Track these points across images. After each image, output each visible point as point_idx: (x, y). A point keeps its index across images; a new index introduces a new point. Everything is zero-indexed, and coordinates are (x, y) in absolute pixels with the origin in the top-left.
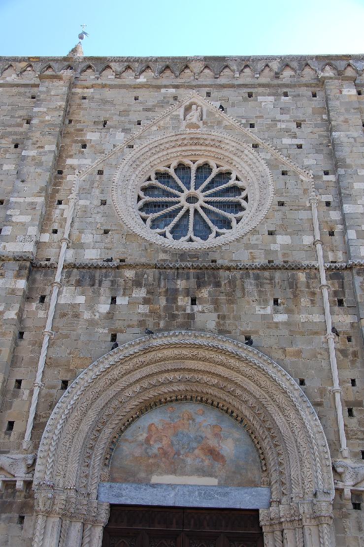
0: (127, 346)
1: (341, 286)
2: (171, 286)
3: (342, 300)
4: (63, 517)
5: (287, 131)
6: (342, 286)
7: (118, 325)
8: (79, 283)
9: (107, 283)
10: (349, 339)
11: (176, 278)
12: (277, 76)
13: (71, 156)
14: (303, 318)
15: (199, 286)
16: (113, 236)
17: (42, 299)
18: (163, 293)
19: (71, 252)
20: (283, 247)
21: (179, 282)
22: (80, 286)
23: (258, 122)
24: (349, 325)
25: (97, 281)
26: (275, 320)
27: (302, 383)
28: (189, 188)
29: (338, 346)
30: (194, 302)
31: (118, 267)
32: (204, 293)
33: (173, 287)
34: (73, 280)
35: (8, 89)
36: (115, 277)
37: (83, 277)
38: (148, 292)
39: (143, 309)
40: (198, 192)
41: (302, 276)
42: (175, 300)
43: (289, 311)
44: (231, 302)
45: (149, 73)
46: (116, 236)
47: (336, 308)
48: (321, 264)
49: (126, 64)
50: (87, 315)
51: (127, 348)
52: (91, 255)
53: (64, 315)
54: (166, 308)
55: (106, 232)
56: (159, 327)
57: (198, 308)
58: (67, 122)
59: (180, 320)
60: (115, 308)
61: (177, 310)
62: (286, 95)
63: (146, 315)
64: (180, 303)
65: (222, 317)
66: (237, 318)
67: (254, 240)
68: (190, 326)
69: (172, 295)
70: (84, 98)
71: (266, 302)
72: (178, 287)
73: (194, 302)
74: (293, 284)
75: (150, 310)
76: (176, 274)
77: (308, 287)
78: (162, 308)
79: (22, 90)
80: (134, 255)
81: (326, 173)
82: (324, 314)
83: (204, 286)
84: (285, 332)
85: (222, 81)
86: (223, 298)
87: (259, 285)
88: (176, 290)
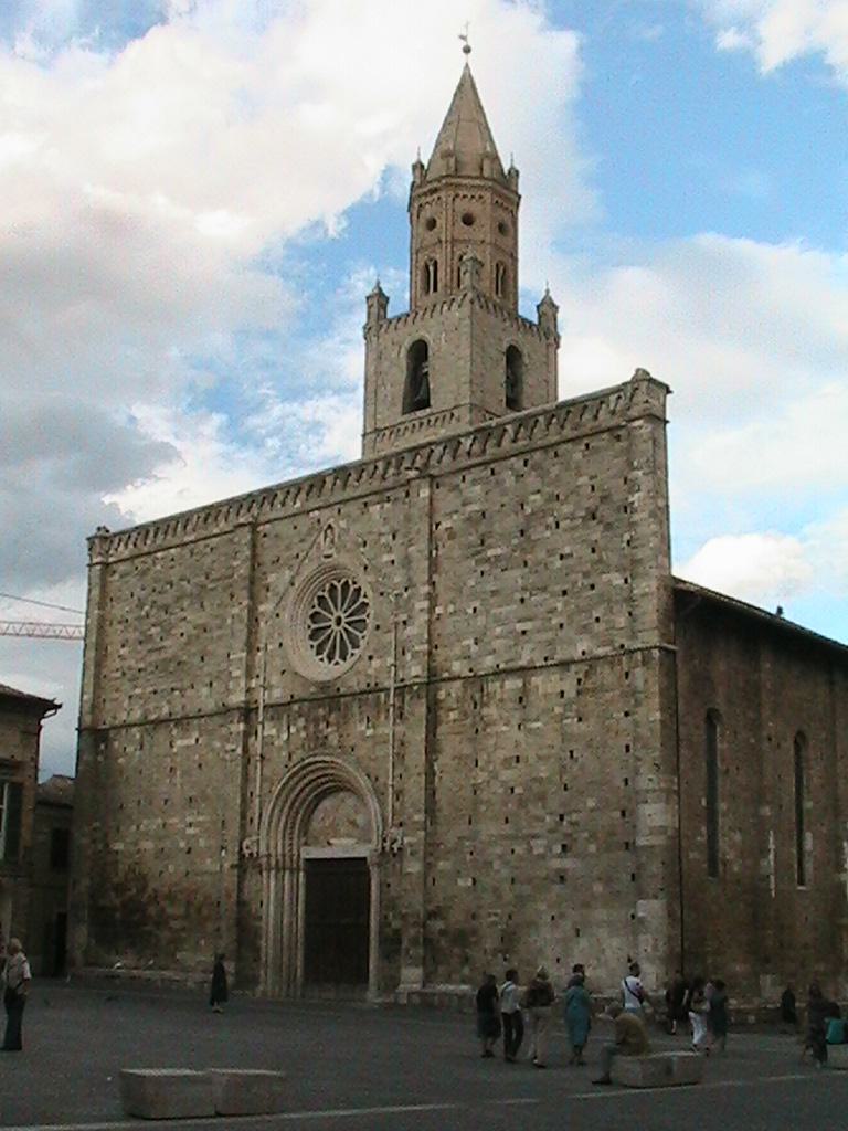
7: (292, 747)
9: (285, 716)
12: (383, 478)
13: (261, 603)
14: (380, 731)
15: (330, 712)
20: (376, 669)
23: (369, 539)
28: (330, 620)
30: (327, 726)
31: (289, 703)
32: (332, 718)
38: (306, 720)
39: (303, 734)
41: (383, 695)
43: (374, 727)
45: (303, 495)
47: (398, 721)
48: (390, 684)
49: (286, 490)
52: (277, 695)
57: (330, 730)
65: (341, 736)
67: (360, 666)
69: (316, 722)
70: (265, 535)
73: (327, 726)
79: (229, 536)
80: (299, 694)
81: (406, 589)
85: (350, 493)
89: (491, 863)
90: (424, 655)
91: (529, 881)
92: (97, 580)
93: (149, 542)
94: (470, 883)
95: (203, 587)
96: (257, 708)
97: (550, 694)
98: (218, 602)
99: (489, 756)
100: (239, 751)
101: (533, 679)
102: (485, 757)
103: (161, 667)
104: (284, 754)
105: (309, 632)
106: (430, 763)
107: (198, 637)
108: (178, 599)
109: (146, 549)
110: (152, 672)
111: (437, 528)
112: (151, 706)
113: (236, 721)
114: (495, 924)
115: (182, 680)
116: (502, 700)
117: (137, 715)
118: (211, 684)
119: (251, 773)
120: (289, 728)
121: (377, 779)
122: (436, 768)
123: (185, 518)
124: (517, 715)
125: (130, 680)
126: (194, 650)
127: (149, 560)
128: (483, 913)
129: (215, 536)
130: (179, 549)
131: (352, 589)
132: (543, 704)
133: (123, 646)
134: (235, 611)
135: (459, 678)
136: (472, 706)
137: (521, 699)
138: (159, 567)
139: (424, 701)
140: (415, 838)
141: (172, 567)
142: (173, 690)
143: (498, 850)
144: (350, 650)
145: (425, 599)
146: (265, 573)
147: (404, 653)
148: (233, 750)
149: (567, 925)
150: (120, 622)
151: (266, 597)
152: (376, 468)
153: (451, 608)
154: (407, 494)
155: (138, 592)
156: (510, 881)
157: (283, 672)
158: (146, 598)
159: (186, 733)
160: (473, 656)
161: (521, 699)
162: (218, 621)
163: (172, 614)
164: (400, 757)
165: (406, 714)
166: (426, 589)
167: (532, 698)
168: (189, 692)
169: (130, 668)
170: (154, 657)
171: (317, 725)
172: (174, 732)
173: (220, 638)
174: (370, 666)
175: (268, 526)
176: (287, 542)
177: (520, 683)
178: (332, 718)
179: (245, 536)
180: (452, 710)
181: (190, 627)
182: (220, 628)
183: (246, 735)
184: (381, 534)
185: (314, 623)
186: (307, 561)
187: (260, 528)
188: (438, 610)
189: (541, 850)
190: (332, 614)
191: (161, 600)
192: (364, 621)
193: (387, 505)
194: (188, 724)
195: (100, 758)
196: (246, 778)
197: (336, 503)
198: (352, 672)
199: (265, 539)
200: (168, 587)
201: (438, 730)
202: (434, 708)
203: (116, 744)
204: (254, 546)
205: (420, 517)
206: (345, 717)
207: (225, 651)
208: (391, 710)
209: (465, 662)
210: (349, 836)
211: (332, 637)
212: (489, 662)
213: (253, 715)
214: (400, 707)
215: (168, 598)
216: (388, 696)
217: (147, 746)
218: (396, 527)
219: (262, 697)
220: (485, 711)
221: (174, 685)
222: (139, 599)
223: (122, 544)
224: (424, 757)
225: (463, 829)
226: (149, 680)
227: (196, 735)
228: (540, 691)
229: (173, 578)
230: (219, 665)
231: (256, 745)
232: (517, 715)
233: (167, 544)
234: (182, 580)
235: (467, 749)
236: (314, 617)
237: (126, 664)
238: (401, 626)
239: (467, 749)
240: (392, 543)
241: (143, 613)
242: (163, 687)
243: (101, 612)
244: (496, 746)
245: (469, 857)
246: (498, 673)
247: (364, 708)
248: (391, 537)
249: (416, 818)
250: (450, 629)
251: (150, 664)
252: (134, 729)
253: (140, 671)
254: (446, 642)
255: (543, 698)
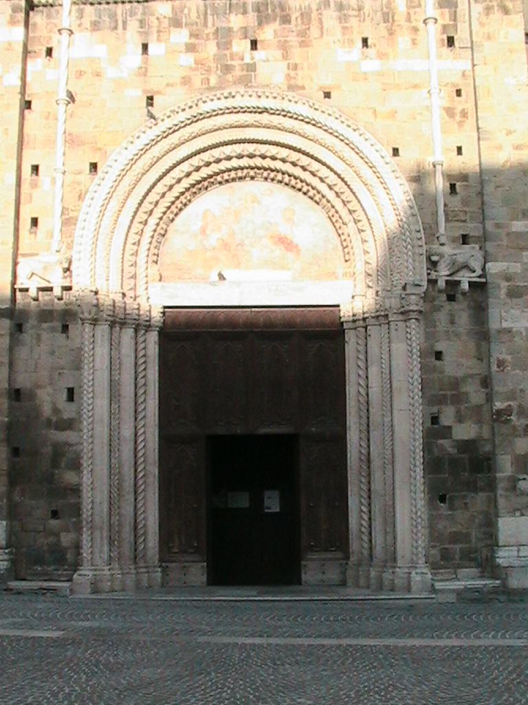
0: (168, 114)
1: (453, 18)
2: (221, 23)
3: (453, 38)
6: (454, 17)
7: (154, 84)
8: (96, 26)
10: (459, 93)
11: (228, 11)
15: (260, 24)
17: (49, 52)
18: (211, 36)
21: (233, 17)
22: (98, 30)
24: (461, 74)
25: (120, 23)
32: (267, 34)
33: (224, 25)
34: (87, 22)
36: (144, 14)
37: (100, 18)
38: (191, 35)
42: (228, 45)
43: (382, 56)
44: (304, 44)
50: (111, 73)
51: (169, 117)
53: (80, 74)
54: (217, 58)
56: (208, 83)
57: (259, 54)
60: (147, 59)
61: (232, 59)
63: (191, 69)
68: (251, 82)
69: (224, 37)
71: (351, 42)
72: (231, 25)
73: (254, 44)
75: (195, 60)
76: (228, 5)
77: (409, 19)
78: (211, 57)
82: (429, 57)
83: (268, 23)
86: (293, 39)
87: (343, 19)
88: (230, 30)
206: (303, 34)
247: (353, 22)
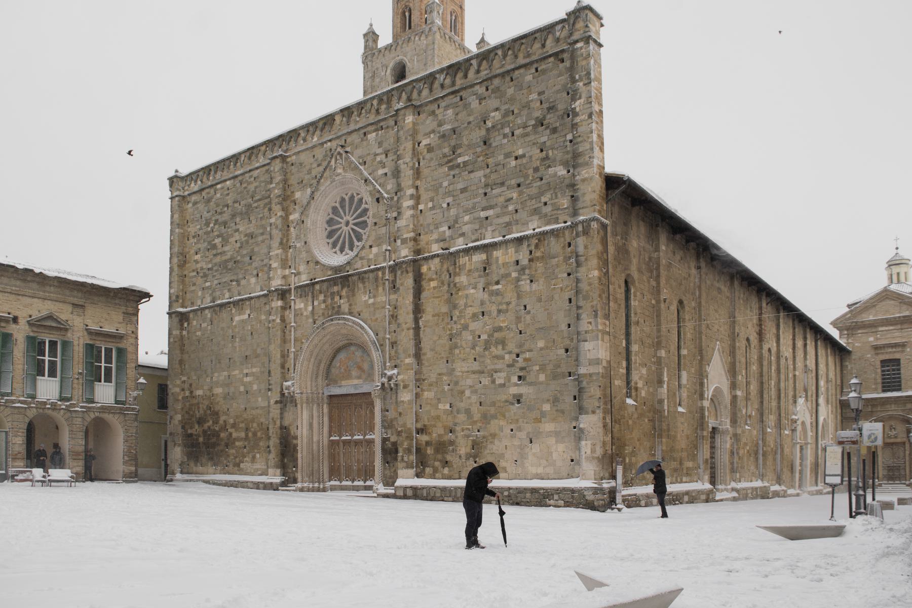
2: (332, 291)
4: (307, 403)
5: (381, 162)
15: (342, 289)
16: (311, 264)
19: (297, 278)
23: (369, 159)
26: (369, 303)
27: (377, 335)
29: (391, 313)
30: (340, 299)
32: (344, 293)
35: (261, 169)
38: (325, 296)
39: (323, 306)
40: (345, 218)
41: (380, 273)
42: (334, 298)
43: (374, 297)
44: (354, 295)
45: (318, 132)
46: (312, 264)
47: (391, 291)
52: (304, 280)
54: (331, 305)
55: (308, 262)
57: (342, 301)
58: (287, 186)
59: (336, 309)
62: (382, 128)
64: (335, 300)
65: (350, 305)
66: (356, 304)
67: (363, 253)
70: (292, 165)
71: (366, 292)
73: (340, 299)
74: (376, 279)
79: (267, 167)
84: (372, 309)
85: (352, 127)
86: (351, 293)
88: (334, 292)
89: (463, 392)
90: (410, 241)
91: (493, 404)
92: (177, 208)
93: (211, 178)
94: (448, 407)
95: (250, 206)
96: (290, 289)
97: (508, 263)
98: (261, 215)
99: (460, 312)
100: (278, 321)
101: (495, 252)
102: (458, 313)
103: (224, 265)
104: (311, 320)
105: (326, 233)
106: (416, 320)
107: (247, 242)
108: (233, 216)
109: (210, 184)
110: (216, 271)
111: (419, 146)
112: (218, 293)
113: (275, 298)
114: (468, 436)
115: (237, 274)
116: (470, 271)
117: (207, 302)
118: (258, 275)
119: (287, 337)
120: (313, 302)
121: (377, 335)
122: (421, 324)
123: (235, 158)
124: (482, 280)
125: (202, 277)
126: (245, 252)
127: (212, 191)
128: (458, 428)
129: (257, 168)
130: (232, 181)
131: (356, 199)
132: (502, 271)
133: (197, 254)
134: (273, 220)
135: (438, 256)
136: (448, 277)
137: (485, 269)
138: (218, 195)
139: (411, 275)
140: (407, 376)
141: (228, 194)
142: (231, 281)
143: (469, 382)
144: (356, 243)
145: (410, 199)
146: (293, 192)
147: (395, 241)
148: (274, 320)
149: (523, 435)
150: (194, 237)
151: (295, 209)
152: (372, 105)
153: (430, 205)
154: (396, 124)
155: (206, 215)
156: (478, 403)
157: (308, 262)
158: (211, 219)
159: (241, 311)
160: (448, 239)
161: (485, 269)
162: (261, 231)
163: (228, 228)
164: (394, 317)
165: (397, 286)
166: (411, 191)
167: (494, 267)
168: (243, 282)
169: (202, 269)
170: (218, 259)
171: (333, 299)
172: (233, 312)
173: (263, 241)
174: (371, 252)
175: (294, 157)
176: (308, 167)
177: (484, 256)
178: (344, 293)
179: (277, 166)
180: (433, 280)
181: (242, 236)
182: (262, 234)
183: (284, 308)
184: (376, 155)
185: (329, 226)
186: (322, 181)
187: (289, 160)
188: (421, 207)
189: (502, 381)
190: (342, 218)
191: (222, 219)
192: (366, 221)
193: (380, 132)
194: (242, 304)
195: (184, 333)
196: (284, 341)
197: (343, 135)
198: (358, 259)
199: (293, 167)
200: (226, 209)
201: (421, 297)
202: (418, 279)
203: (195, 323)
204: (285, 174)
205: (406, 138)
206: (353, 291)
207: (266, 251)
208: (387, 282)
209: (442, 245)
210: (359, 378)
211: (343, 235)
212: (459, 245)
213: (288, 295)
214: (392, 281)
215: (226, 217)
216: (384, 274)
217: (215, 322)
218: (389, 148)
219: (294, 282)
220: (457, 280)
221: (232, 278)
222: (206, 220)
223: (193, 182)
224: (411, 316)
225: (442, 367)
226: (214, 276)
227: (248, 312)
228: (500, 262)
229: (229, 202)
230: (263, 260)
231: (290, 316)
232: (482, 280)
233: (223, 179)
234: (235, 202)
235: (444, 309)
236: (330, 222)
237: (199, 266)
238: (392, 221)
239: (444, 309)
240: (384, 160)
241: (209, 229)
242: (224, 281)
243: (182, 231)
244: (466, 305)
245: (446, 388)
246: (467, 251)
247: (367, 284)
248: (384, 156)
249: (408, 361)
250: (429, 220)
251: (216, 264)
252: (207, 311)
253: (209, 269)
254: (426, 230)
255: (502, 267)
